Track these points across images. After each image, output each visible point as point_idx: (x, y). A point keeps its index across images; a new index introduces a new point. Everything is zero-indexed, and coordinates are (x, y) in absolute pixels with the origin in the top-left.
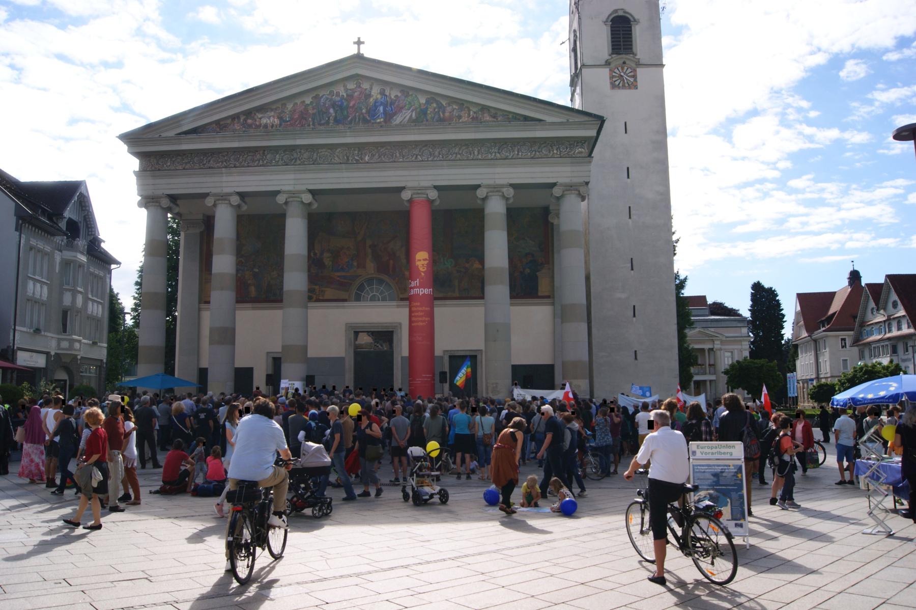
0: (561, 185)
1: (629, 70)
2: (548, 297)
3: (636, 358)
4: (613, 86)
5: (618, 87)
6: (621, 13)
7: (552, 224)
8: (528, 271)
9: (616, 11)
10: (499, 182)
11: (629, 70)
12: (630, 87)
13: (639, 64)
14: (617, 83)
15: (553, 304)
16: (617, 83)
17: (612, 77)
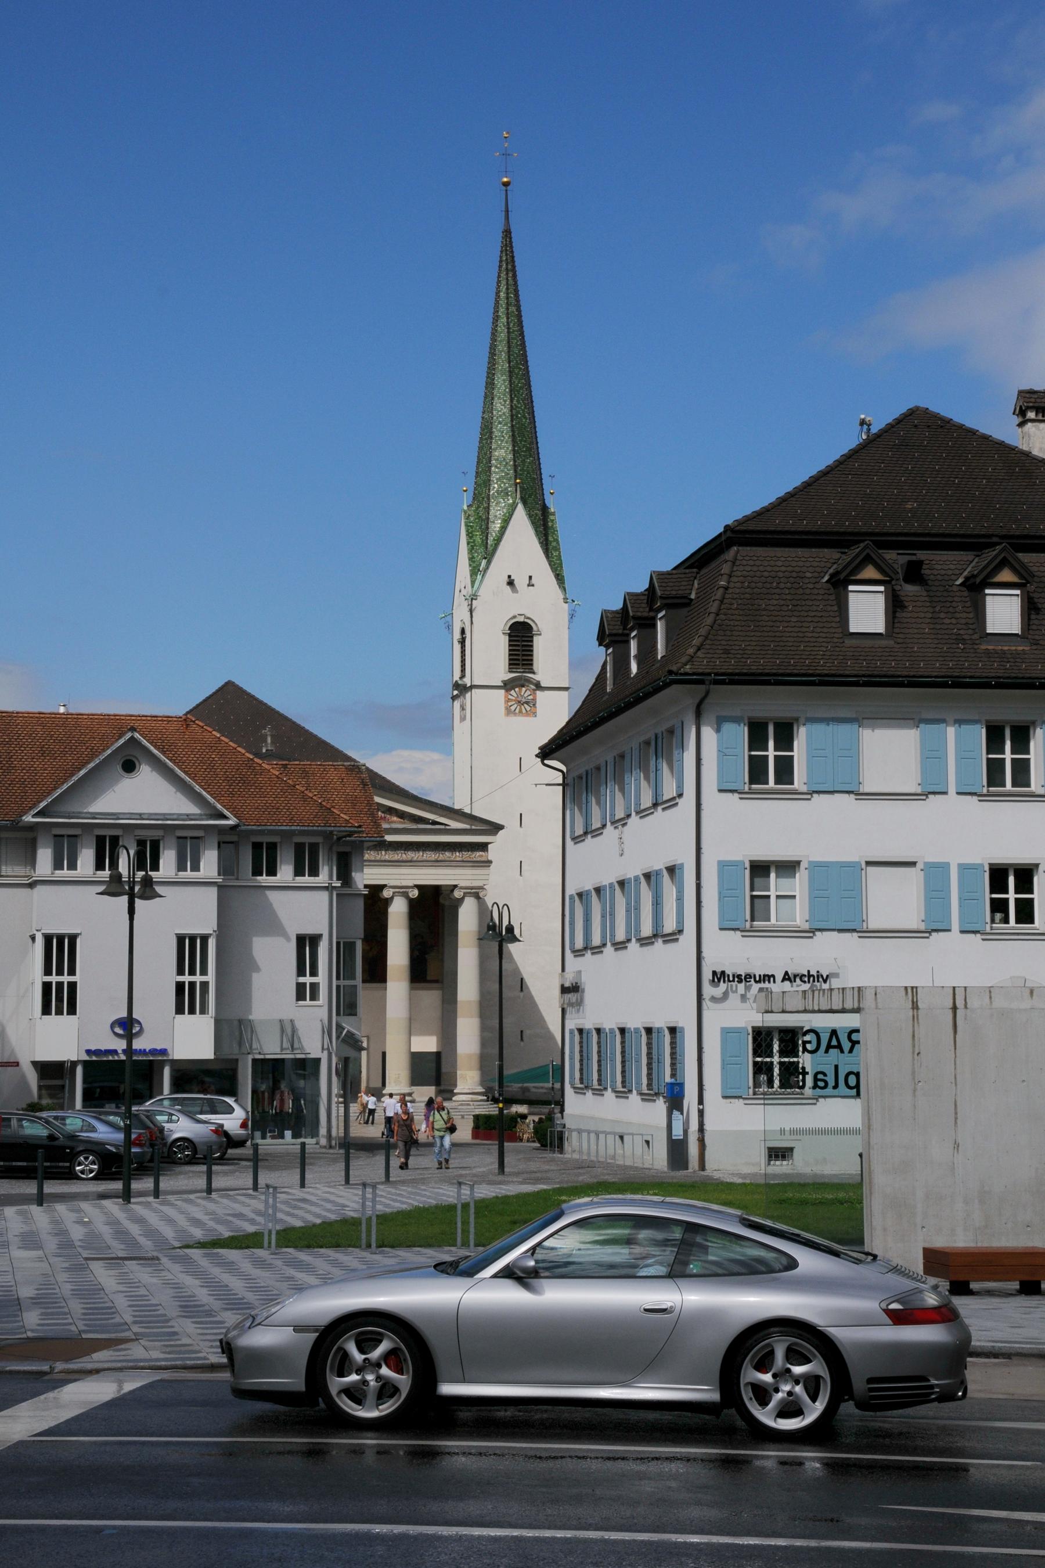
0: (462, 888)
1: (528, 693)
2: (437, 981)
3: (522, 1039)
4: (509, 712)
5: (514, 713)
6: (521, 619)
7: (443, 905)
8: (417, 953)
9: (514, 617)
10: (404, 883)
11: (528, 693)
12: (527, 714)
13: (538, 686)
14: (513, 708)
15: (442, 989)
16: (513, 708)
17: (508, 700)
